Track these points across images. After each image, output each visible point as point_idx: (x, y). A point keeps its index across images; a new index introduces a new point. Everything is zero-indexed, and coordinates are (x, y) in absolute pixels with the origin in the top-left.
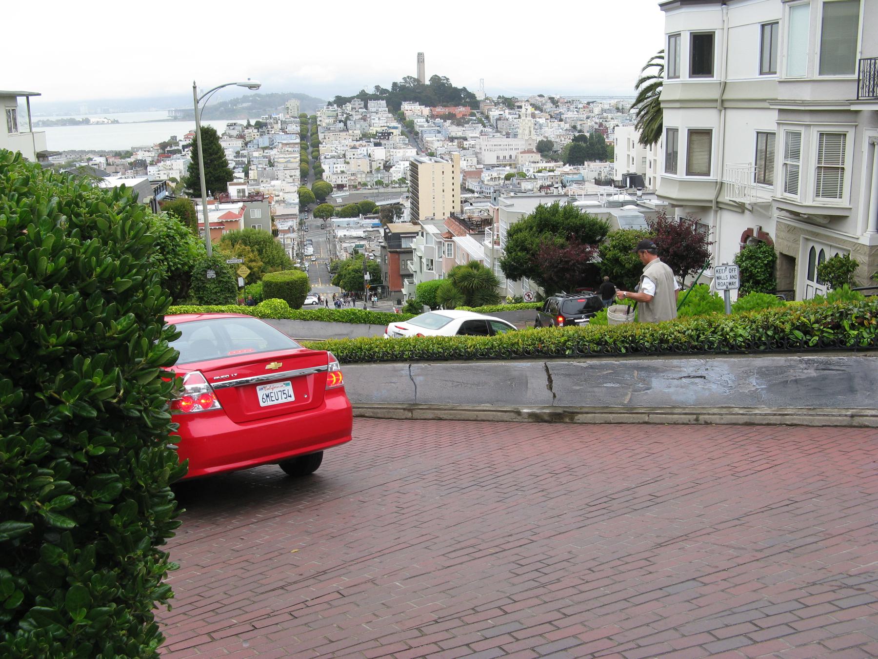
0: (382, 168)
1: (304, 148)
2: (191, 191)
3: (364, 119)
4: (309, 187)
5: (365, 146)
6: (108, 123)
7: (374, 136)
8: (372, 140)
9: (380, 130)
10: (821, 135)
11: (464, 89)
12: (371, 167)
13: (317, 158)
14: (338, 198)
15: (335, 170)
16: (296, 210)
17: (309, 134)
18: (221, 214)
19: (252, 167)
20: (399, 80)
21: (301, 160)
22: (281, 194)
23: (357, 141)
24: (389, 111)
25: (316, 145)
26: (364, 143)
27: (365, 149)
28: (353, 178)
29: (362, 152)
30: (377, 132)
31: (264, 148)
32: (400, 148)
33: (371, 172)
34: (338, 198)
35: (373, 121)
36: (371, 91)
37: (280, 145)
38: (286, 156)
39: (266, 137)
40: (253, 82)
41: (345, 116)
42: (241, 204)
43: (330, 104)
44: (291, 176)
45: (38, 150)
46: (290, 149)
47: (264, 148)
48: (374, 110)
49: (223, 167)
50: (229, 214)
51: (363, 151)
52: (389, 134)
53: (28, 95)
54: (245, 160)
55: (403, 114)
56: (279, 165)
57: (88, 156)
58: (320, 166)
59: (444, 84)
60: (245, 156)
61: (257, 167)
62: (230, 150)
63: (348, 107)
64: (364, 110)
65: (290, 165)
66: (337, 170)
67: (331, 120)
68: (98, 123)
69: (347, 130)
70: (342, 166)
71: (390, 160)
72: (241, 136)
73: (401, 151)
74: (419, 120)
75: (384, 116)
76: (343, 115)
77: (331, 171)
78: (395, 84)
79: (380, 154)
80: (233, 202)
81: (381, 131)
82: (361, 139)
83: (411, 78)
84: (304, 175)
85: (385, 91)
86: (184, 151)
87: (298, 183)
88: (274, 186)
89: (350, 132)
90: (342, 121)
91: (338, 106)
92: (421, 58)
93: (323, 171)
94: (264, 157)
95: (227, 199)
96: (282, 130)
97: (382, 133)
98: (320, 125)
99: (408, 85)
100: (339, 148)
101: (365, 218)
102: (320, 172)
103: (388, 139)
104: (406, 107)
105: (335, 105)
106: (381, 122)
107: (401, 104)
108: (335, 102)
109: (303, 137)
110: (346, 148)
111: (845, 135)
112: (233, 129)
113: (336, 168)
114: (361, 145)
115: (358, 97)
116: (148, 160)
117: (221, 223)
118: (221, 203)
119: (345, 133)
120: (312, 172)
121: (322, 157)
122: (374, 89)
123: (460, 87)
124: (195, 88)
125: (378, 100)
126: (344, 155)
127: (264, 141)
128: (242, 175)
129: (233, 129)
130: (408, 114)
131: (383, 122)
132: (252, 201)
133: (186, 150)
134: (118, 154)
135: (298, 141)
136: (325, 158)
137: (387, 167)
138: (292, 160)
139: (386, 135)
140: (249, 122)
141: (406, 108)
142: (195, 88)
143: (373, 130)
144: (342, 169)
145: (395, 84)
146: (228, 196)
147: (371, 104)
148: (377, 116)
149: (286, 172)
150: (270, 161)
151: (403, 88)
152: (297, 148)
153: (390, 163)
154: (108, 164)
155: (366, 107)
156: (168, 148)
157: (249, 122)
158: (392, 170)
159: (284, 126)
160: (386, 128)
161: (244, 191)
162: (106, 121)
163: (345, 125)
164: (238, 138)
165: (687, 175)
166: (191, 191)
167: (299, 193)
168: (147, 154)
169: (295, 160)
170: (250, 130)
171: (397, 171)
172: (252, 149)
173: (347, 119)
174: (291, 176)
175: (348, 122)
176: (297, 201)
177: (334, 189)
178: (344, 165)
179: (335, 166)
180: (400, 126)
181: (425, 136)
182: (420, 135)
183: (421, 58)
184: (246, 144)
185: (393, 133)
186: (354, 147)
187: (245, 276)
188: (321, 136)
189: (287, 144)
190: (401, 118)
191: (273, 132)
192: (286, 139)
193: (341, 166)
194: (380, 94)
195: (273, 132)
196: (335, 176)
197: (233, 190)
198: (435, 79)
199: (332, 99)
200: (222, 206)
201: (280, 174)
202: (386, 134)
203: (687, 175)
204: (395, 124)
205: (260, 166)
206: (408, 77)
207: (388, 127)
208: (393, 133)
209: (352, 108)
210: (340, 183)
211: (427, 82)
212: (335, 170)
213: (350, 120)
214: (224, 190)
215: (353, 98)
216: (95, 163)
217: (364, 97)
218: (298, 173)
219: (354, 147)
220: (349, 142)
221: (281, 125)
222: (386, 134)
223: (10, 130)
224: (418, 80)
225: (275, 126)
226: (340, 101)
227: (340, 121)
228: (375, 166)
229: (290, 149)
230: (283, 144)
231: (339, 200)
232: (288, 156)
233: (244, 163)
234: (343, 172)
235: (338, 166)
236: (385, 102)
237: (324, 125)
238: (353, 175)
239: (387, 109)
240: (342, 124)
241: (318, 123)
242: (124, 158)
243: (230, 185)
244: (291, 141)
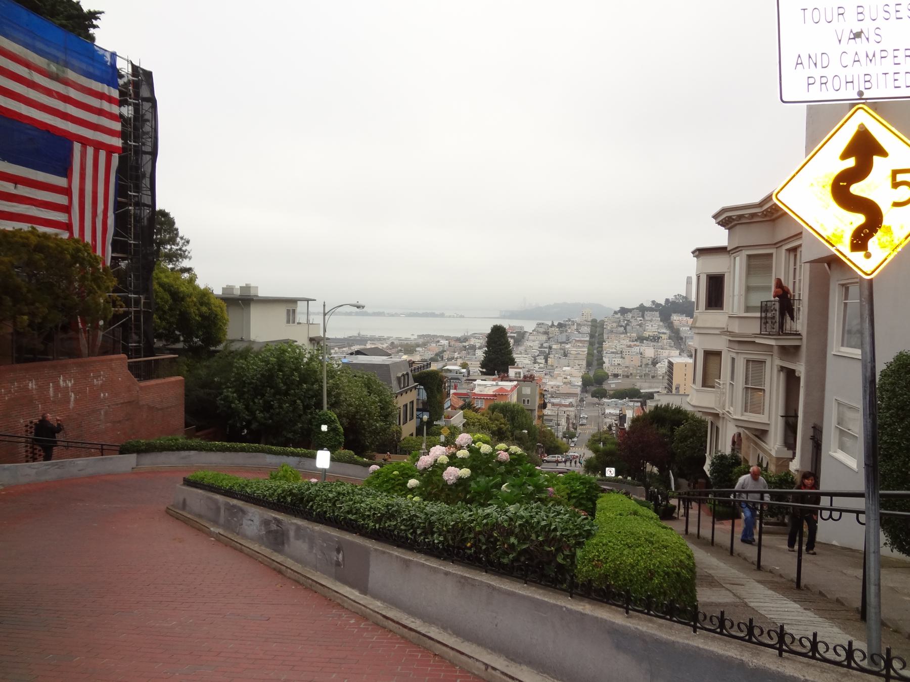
0: (650, 363)
1: (591, 344)
2: (484, 370)
3: (640, 325)
4: (591, 374)
5: (638, 346)
6: (457, 317)
7: (647, 339)
8: (645, 341)
9: (651, 334)
10: (748, 361)
12: (641, 362)
13: (600, 352)
14: (612, 385)
16: (578, 390)
17: (597, 335)
18: (497, 388)
19: (551, 356)
20: (671, 297)
21: (588, 354)
22: (568, 377)
23: (633, 341)
24: (661, 321)
25: (601, 343)
26: (638, 343)
27: (638, 348)
28: (626, 370)
29: (635, 350)
30: (649, 336)
31: (561, 343)
32: (666, 349)
33: (641, 366)
34: (612, 385)
35: (647, 328)
36: (648, 304)
37: (574, 341)
39: (565, 334)
40: (361, 303)
41: (626, 322)
42: (515, 383)
43: (616, 313)
44: (579, 365)
45: (312, 336)
47: (561, 343)
48: (649, 319)
49: (508, 354)
50: (502, 389)
51: (637, 349)
52: (659, 338)
53: (308, 300)
54: (547, 350)
55: (672, 323)
57: (437, 339)
58: (602, 359)
60: (546, 348)
61: (554, 356)
63: (629, 316)
64: (641, 319)
67: (615, 325)
68: (450, 317)
69: (626, 333)
70: (619, 360)
72: (546, 333)
73: (667, 351)
74: (684, 328)
75: (657, 323)
77: (610, 363)
78: (667, 300)
79: (649, 352)
80: (511, 381)
82: (636, 340)
83: (681, 295)
84: (589, 364)
85: (658, 305)
87: (583, 370)
88: (565, 371)
89: (628, 334)
90: (623, 326)
91: (621, 315)
93: (604, 363)
94: (561, 349)
95: (505, 378)
96: (577, 330)
97: (653, 337)
100: (618, 346)
101: (631, 401)
102: (601, 363)
103: (658, 342)
104: (676, 318)
105: (619, 314)
106: (653, 328)
107: (671, 315)
108: (619, 311)
109: (592, 336)
110: (623, 346)
111: (765, 362)
114: (635, 345)
115: (637, 308)
116: (478, 345)
117: (495, 396)
118: (502, 381)
119: (623, 336)
120: (595, 363)
121: (605, 352)
122: (650, 303)
124: (324, 306)
125: (653, 311)
126: (622, 352)
127: (563, 338)
128: (543, 361)
130: (676, 323)
131: (655, 328)
132: (524, 381)
134: (458, 340)
135: (588, 339)
136: (607, 353)
137: (655, 363)
138: (582, 353)
139: (656, 339)
140: (553, 323)
141: (675, 319)
142: (324, 306)
143: (646, 334)
145: (667, 300)
146: (508, 376)
148: (651, 323)
149: (575, 361)
150: (564, 352)
151: (673, 303)
152: (587, 345)
154: (450, 346)
155: (643, 316)
157: (553, 323)
158: (657, 366)
161: (520, 373)
162: (455, 315)
163: (625, 329)
165: (702, 387)
166: (484, 370)
167: (583, 377)
168: (477, 341)
169: (582, 353)
170: (553, 329)
171: (662, 367)
172: (553, 343)
173: (627, 324)
174: (579, 365)
175: (628, 328)
176: (580, 383)
177: (610, 377)
179: (613, 359)
180: (668, 332)
181: (687, 341)
184: (549, 338)
186: (630, 346)
187: (446, 434)
188: (605, 336)
189: (578, 341)
190: (670, 326)
193: (618, 360)
194: (656, 307)
196: (612, 368)
197: (512, 372)
199: (618, 309)
200: (500, 383)
201: (571, 363)
203: (702, 387)
204: (664, 331)
205: (557, 355)
207: (659, 332)
209: (632, 317)
210: (616, 373)
212: (613, 362)
214: (507, 372)
215: (633, 309)
216: (442, 344)
217: (642, 309)
218: (584, 363)
219: (630, 346)
220: (627, 342)
223: (288, 322)
224: (686, 298)
225: (572, 327)
226: (624, 311)
227: (621, 326)
228: (645, 361)
229: (580, 345)
230: (576, 340)
231: (613, 386)
233: (545, 352)
234: (619, 364)
236: (657, 314)
237: (609, 328)
238: (627, 367)
239: (659, 319)
240: (623, 328)
241: (605, 327)
242: (461, 342)
243: (511, 368)
244: (583, 339)
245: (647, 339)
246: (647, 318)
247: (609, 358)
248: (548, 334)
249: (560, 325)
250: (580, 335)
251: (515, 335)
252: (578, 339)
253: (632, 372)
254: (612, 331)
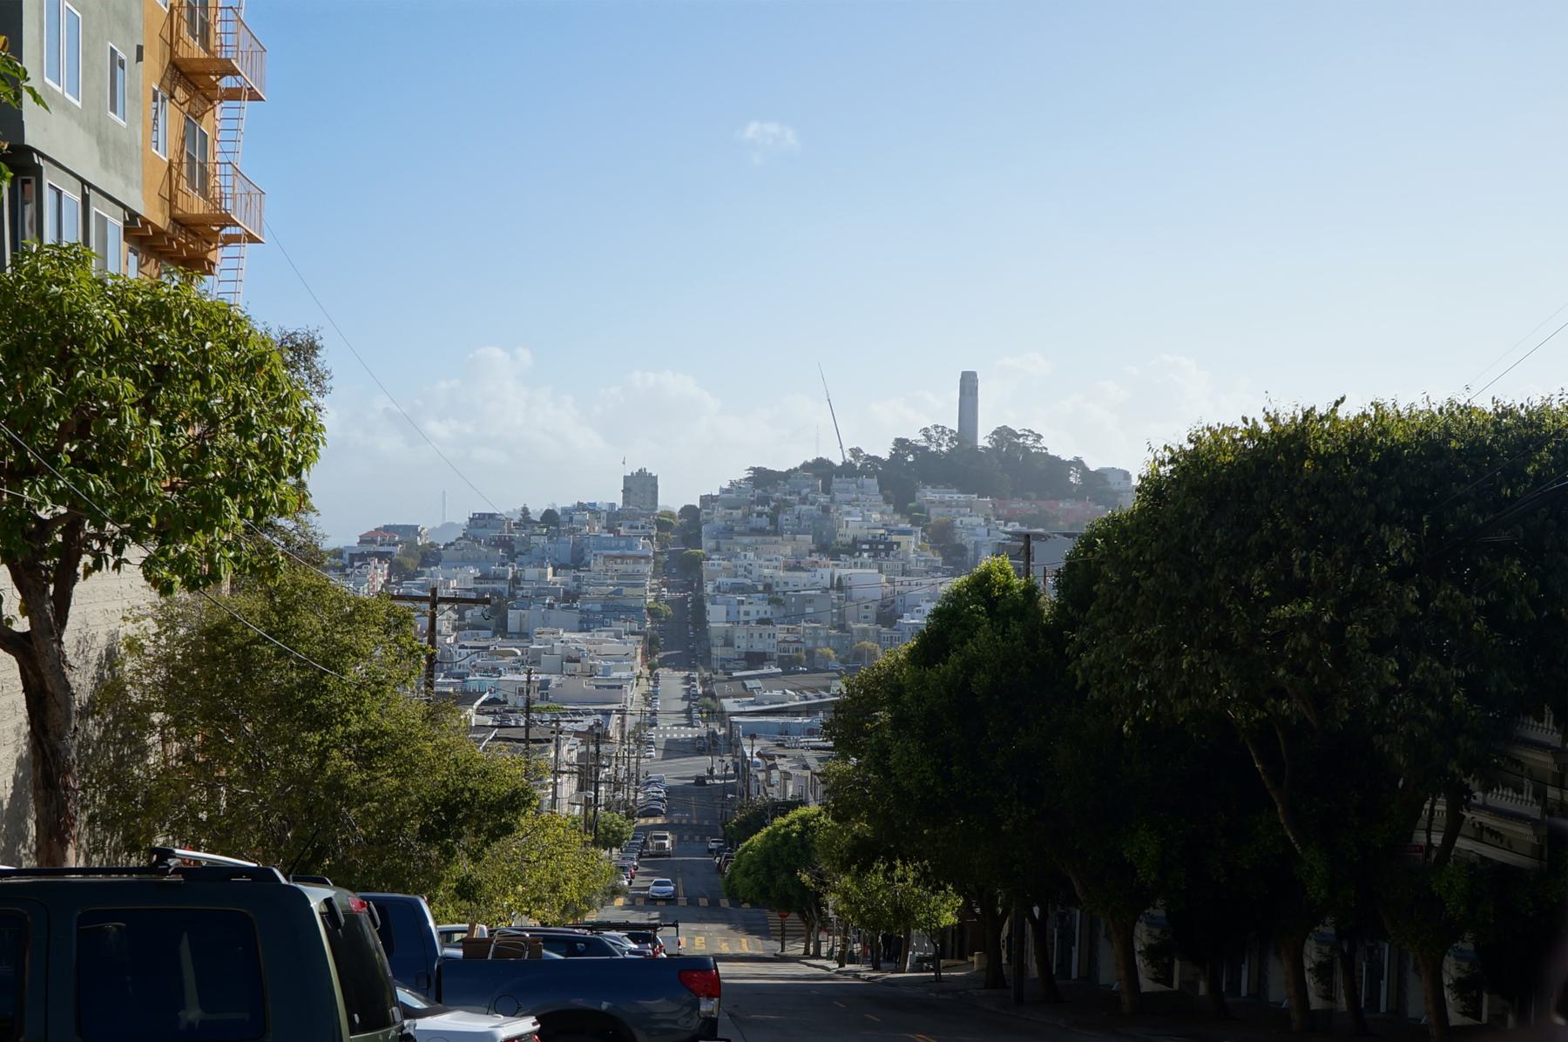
7: (853, 548)
11: (1078, 463)
15: (743, 618)
20: (915, 436)
27: (826, 573)
48: (848, 497)
59: (1026, 449)
66: (746, 618)
67: (738, 514)
69: (777, 532)
71: (893, 601)
78: (901, 443)
81: (870, 538)
92: (969, 384)
98: (707, 522)
99: (933, 448)
104: (929, 494)
113: (747, 613)
123: (1067, 457)
139: (881, 548)
144: (762, 615)
145: (901, 443)
147: (837, 483)
153: (894, 610)
155: (827, 490)
160: (882, 531)
163: (773, 520)
173: (777, 510)
175: (782, 518)
178: (768, 608)
179: (743, 608)
182: (971, 553)
183: (969, 384)
185: (898, 544)
198: (1004, 435)
202: (881, 547)
206: (937, 427)
208: (898, 544)
211: (983, 441)
213: (785, 512)
222: (881, 547)
235: (752, 609)
245: (853, 548)
246: (839, 496)
247: (728, 604)
249: (549, 517)
253: (810, 644)
254: (732, 530)
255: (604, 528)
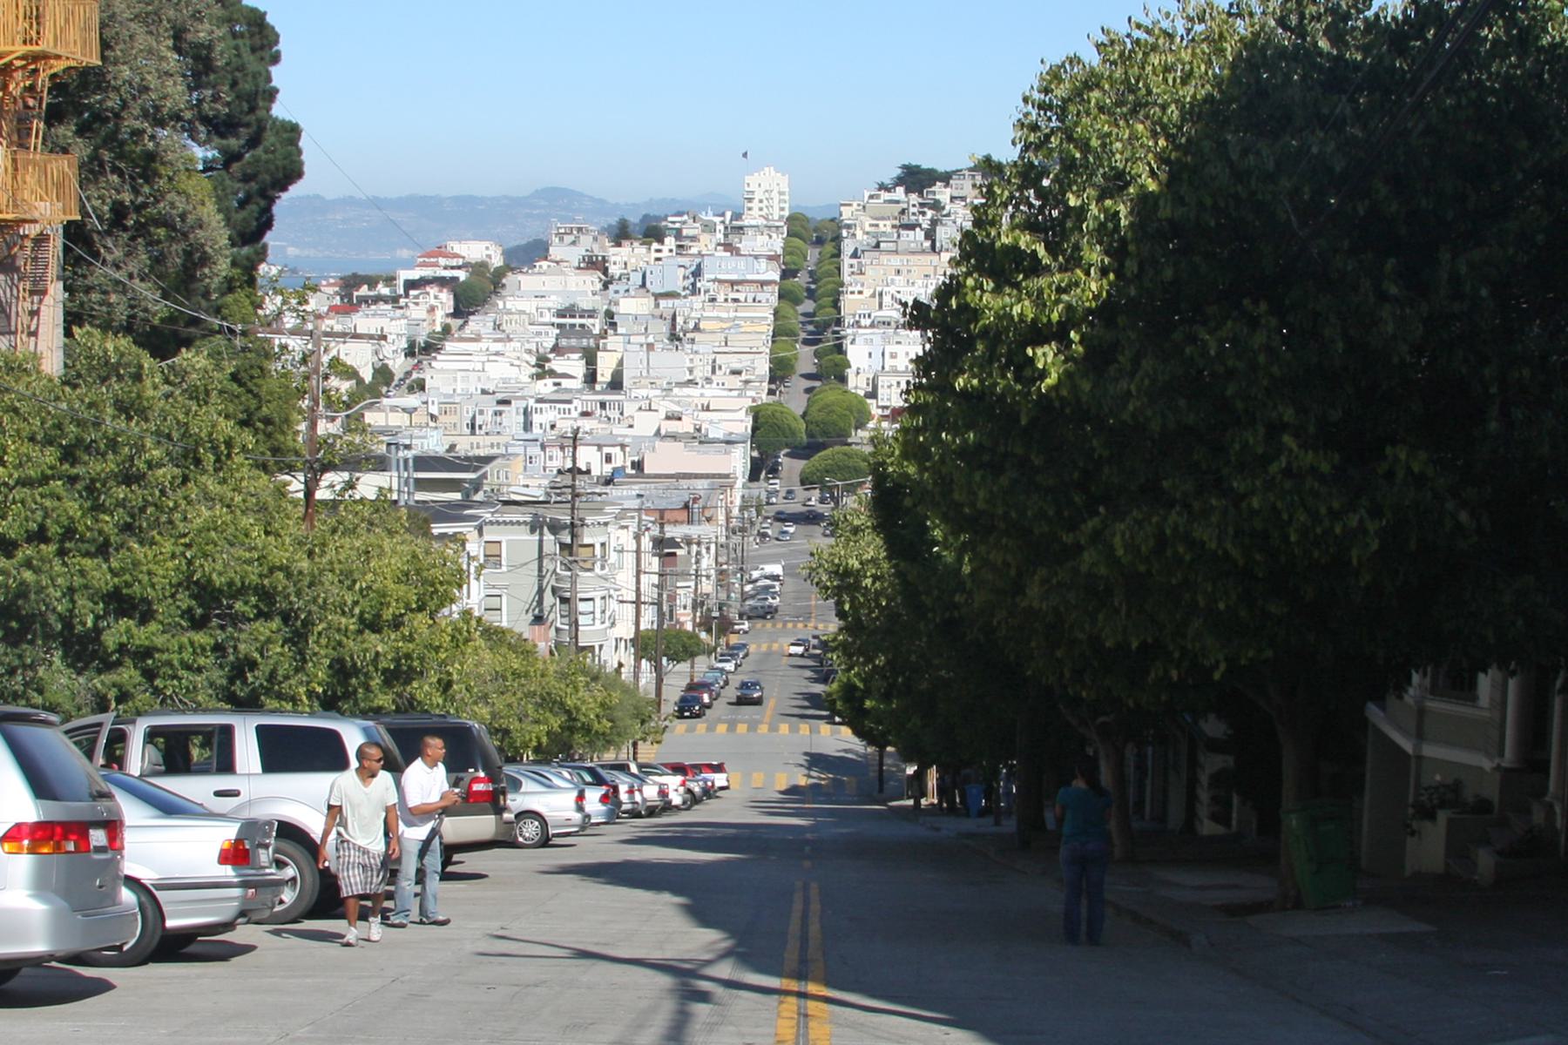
38: (724, 315)
46: (741, 296)
56: (697, 336)
62: (553, 298)
65: (738, 343)
67: (886, 226)
76: (924, 214)
86: (407, 296)
96: (728, 247)
112: (574, 243)
129: (574, 243)
133: (412, 293)
135: (775, 276)
138: (747, 327)
152: (770, 297)
156: (364, 290)
159: (734, 239)
163: (930, 235)
164: (587, 268)
173: (934, 222)
189: (733, 283)
191: (694, 251)
192: (731, 268)
195: (694, 251)
218: (763, 367)
221: (726, 236)
227: (911, 227)
230: (721, 282)
232: (732, 314)
240: (920, 234)
244: (749, 277)
248: (605, 271)
250: (741, 263)
251: (462, 275)
252: (734, 277)
255: (719, 244)
